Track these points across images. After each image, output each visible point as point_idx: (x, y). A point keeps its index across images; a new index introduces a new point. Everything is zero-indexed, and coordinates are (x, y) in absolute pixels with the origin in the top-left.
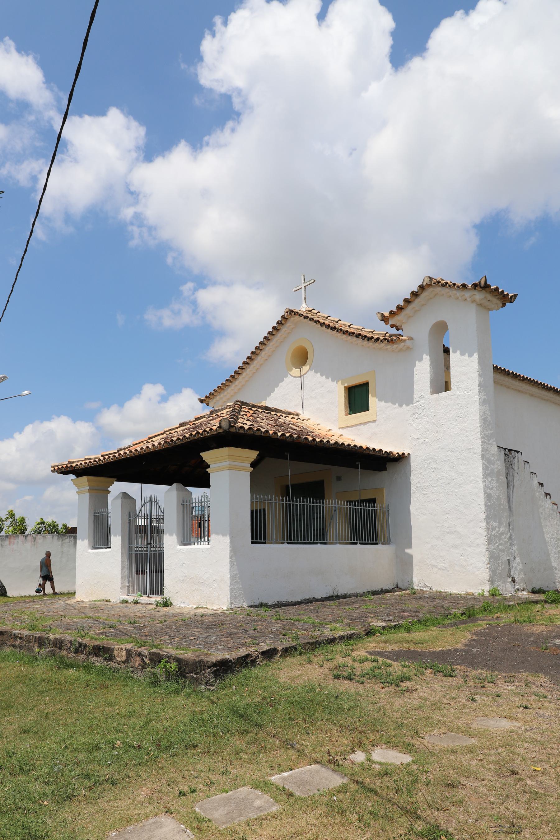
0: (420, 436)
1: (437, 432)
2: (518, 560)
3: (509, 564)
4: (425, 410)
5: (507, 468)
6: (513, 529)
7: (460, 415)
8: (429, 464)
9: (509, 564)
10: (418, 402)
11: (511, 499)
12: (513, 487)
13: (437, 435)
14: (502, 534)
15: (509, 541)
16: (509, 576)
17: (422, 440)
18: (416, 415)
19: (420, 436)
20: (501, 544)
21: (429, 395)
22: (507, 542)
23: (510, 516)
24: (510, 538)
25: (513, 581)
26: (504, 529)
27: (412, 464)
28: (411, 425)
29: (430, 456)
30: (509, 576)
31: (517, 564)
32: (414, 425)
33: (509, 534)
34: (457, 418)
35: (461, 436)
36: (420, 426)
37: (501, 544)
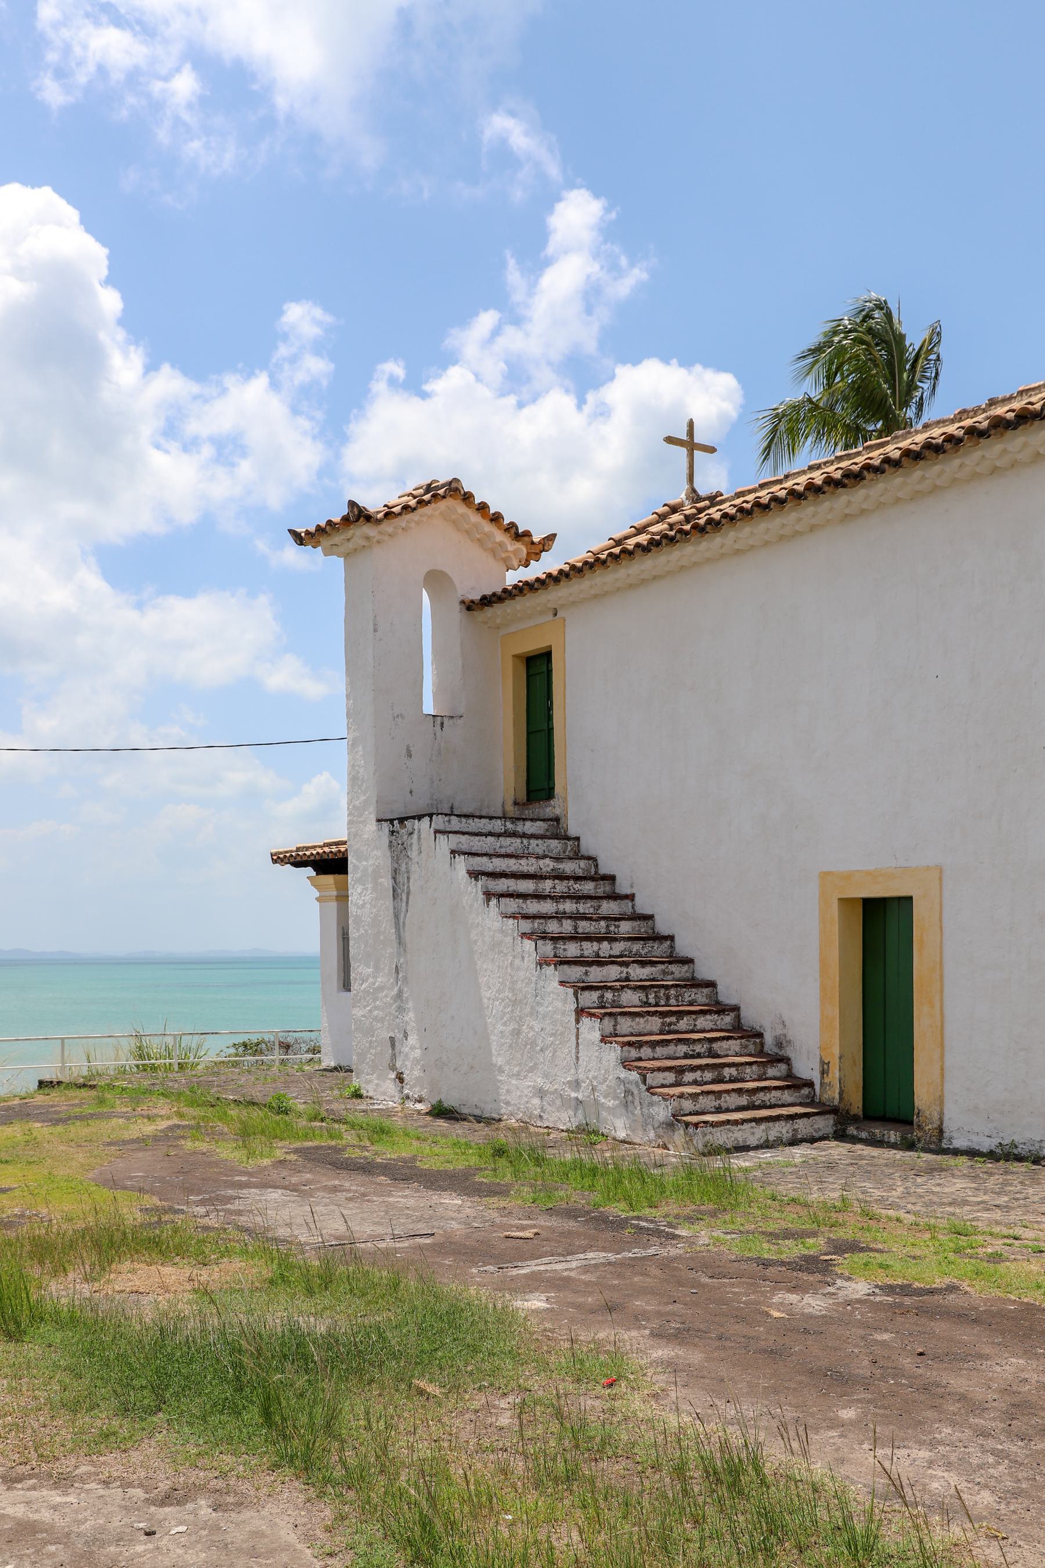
2: (412, 1040)
3: (393, 1045)
5: (396, 860)
6: (405, 978)
9: (393, 1045)
11: (401, 921)
12: (408, 894)
14: (381, 988)
15: (395, 1001)
16: (393, 1068)
20: (376, 1008)
22: (391, 1005)
23: (399, 954)
24: (400, 995)
25: (400, 1078)
26: (384, 980)
30: (393, 1068)
31: (412, 1049)
33: (396, 989)
37: (376, 1008)
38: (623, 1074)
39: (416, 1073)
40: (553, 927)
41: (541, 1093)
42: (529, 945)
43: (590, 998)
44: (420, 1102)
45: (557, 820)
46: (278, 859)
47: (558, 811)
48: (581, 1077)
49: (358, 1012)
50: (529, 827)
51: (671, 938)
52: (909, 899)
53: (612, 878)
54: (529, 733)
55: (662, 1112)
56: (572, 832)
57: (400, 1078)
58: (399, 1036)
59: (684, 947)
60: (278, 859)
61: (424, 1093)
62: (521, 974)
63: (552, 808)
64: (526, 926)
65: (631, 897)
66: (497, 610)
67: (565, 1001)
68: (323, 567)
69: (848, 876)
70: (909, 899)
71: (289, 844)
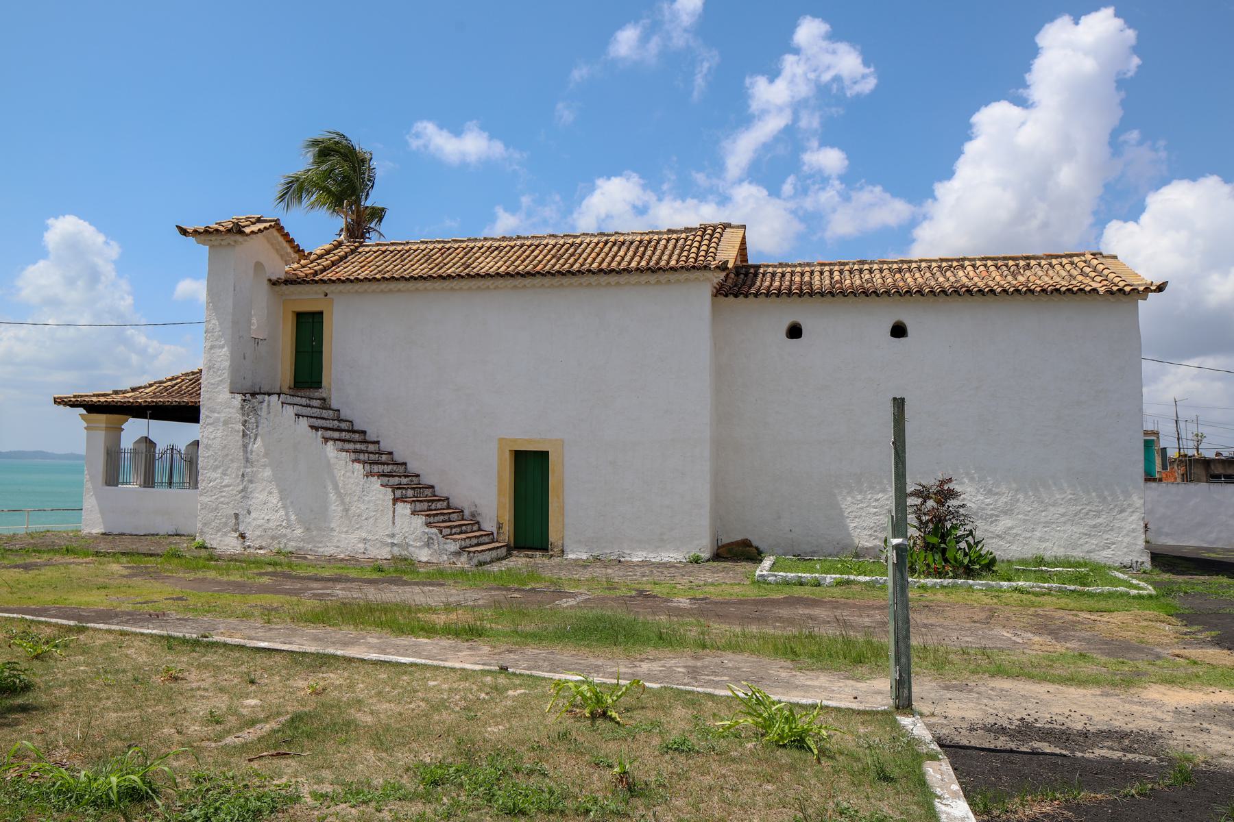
16: (236, 531)
24: (244, 490)
25: (243, 536)
38: (427, 530)
39: (257, 533)
40: (362, 457)
41: (365, 540)
42: (358, 466)
43: (398, 493)
44: (261, 548)
45: (324, 399)
46: (59, 401)
47: (324, 395)
48: (396, 530)
49: (205, 499)
50: (316, 403)
51: (405, 464)
52: (547, 452)
53: (364, 432)
54: (297, 352)
55: (453, 547)
56: (334, 405)
57: (243, 536)
58: (242, 512)
59: (413, 467)
60: (59, 401)
61: (264, 544)
62: (352, 481)
63: (322, 393)
64: (353, 456)
65: (378, 442)
66: (292, 288)
67: (385, 494)
68: (200, 251)
69: (515, 441)
70: (547, 452)
71: (68, 393)
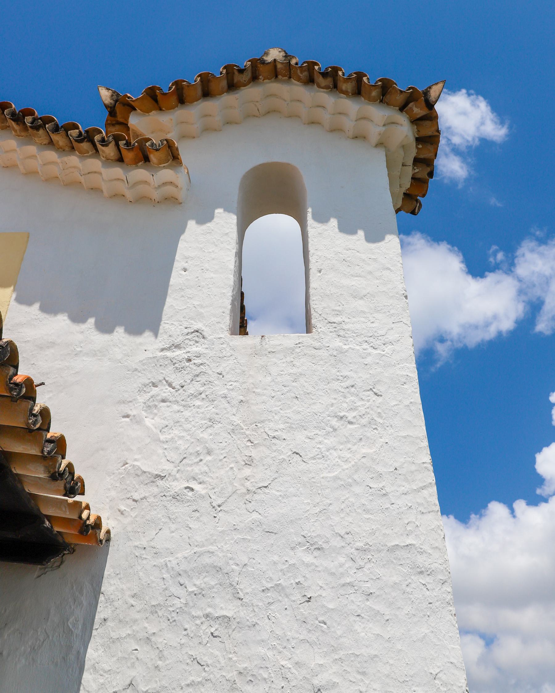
0: (168, 467)
1: (249, 462)
4: (202, 379)
7: (350, 416)
8: (200, 594)
10: (178, 347)
13: (247, 471)
17: (178, 486)
18: (164, 391)
19: (168, 467)
21: (225, 335)
27: (109, 586)
28: (137, 421)
29: (207, 560)
32: (148, 422)
34: (334, 422)
35: (357, 489)
36: (176, 432)
